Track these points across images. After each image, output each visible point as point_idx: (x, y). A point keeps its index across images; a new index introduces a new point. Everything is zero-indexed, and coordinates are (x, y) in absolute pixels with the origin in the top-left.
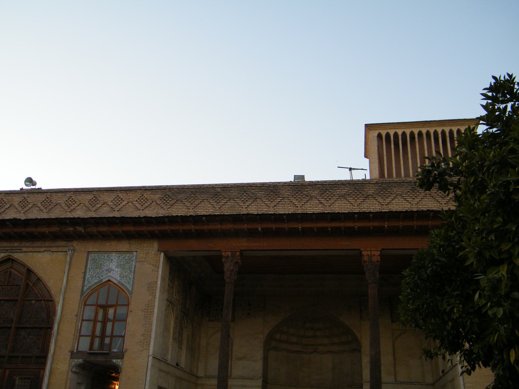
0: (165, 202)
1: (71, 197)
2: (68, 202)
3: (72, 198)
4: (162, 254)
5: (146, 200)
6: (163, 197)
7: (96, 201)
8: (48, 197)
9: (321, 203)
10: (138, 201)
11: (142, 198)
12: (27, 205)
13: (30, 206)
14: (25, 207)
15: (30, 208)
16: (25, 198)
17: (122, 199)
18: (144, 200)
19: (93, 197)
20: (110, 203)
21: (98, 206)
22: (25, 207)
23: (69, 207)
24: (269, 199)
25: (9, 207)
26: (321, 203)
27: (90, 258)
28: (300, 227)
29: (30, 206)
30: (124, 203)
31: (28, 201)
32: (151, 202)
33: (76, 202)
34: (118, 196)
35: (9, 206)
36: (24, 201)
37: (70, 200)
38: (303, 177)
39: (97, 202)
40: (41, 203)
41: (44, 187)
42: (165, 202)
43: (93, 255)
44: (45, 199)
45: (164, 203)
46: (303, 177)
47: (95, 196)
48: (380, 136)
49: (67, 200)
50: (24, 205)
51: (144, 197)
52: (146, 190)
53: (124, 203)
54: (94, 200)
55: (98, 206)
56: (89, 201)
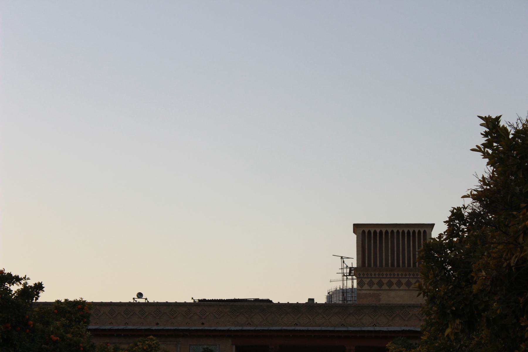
0: (232, 314)
1: (173, 309)
2: (171, 312)
3: (174, 310)
4: (234, 346)
5: (221, 312)
6: (231, 310)
7: (189, 312)
8: (157, 309)
9: (324, 318)
10: (216, 312)
11: (219, 311)
12: (145, 313)
13: (147, 314)
14: (143, 314)
15: (147, 315)
16: (142, 309)
17: (206, 311)
18: (220, 312)
19: (187, 309)
20: (199, 314)
21: (191, 315)
22: (143, 314)
23: (172, 316)
24: (295, 314)
25: (133, 314)
26: (324, 318)
27: (191, 348)
28: (313, 335)
29: (147, 314)
30: (207, 314)
31: (145, 311)
32: (224, 313)
33: (176, 312)
34: (203, 309)
35: (133, 314)
36: (142, 311)
37: (173, 311)
38: (313, 300)
39: (190, 312)
40: (154, 312)
41: (151, 300)
42: (232, 314)
43: (192, 346)
44: (156, 310)
45: (232, 314)
46: (313, 300)
47: (188, 309)
48: (364, 232)
49: (170, 311)
50: (142, 313)
51: (220, 310)
52: (221, 305)
53: (207, 314)
54: (188, 311)
55: (191, 315)
56: (185, 312)
